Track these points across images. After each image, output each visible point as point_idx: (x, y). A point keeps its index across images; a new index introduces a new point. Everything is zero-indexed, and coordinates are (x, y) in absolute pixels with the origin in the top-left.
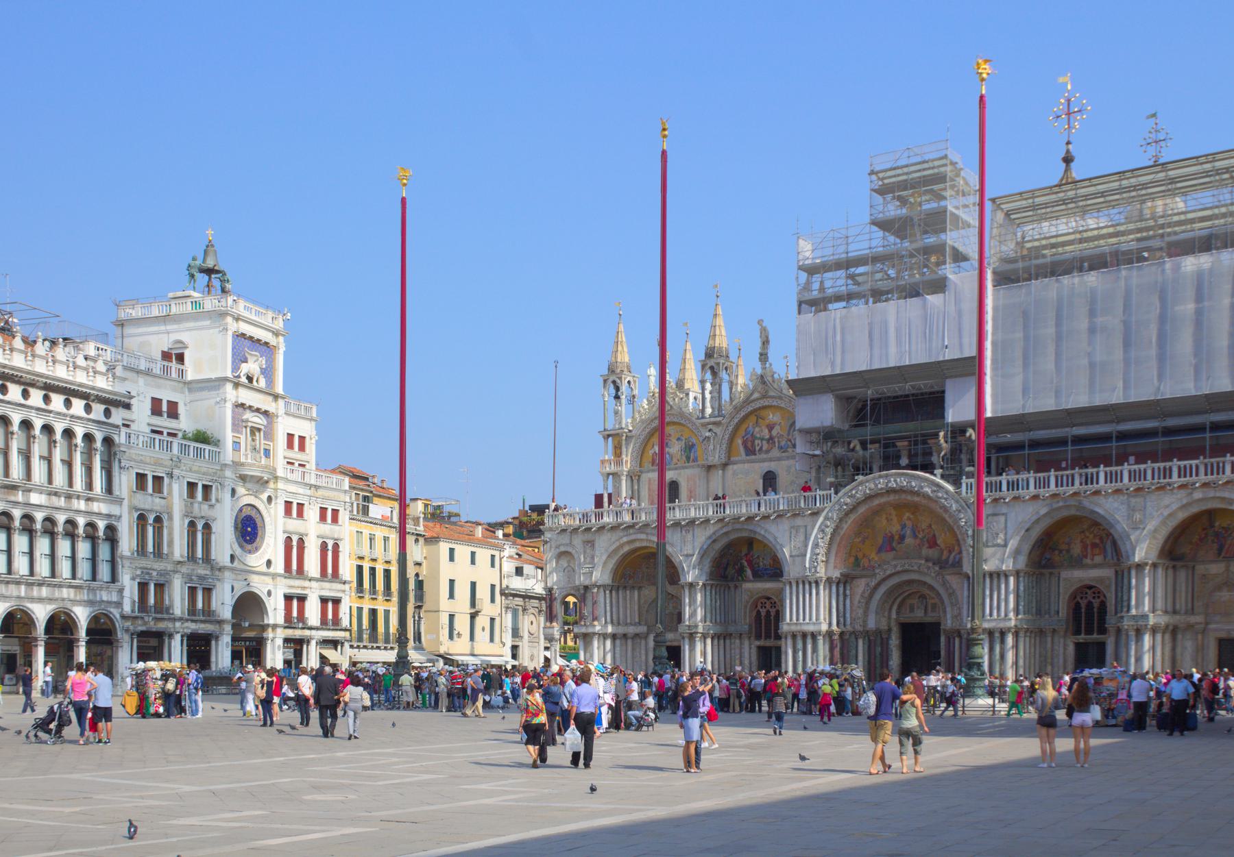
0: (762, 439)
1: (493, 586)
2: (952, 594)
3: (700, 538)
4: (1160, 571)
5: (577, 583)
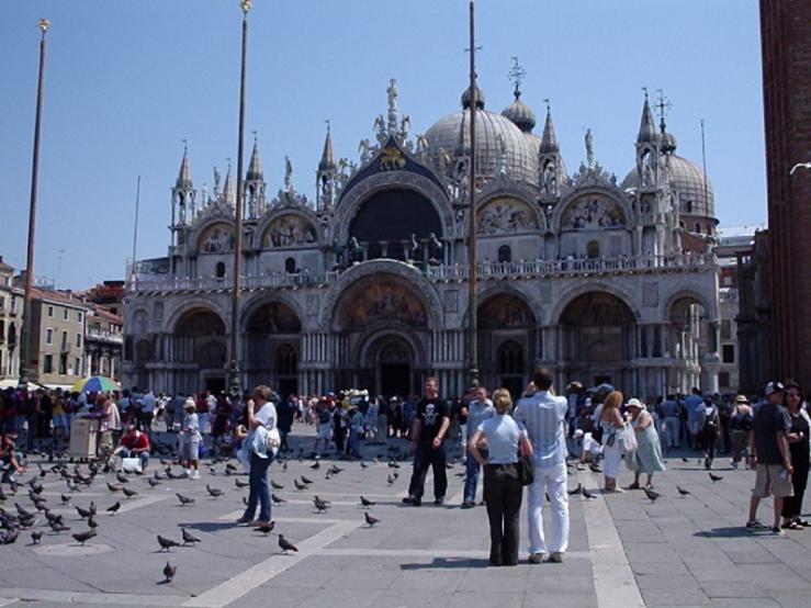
0: (285, 236)
1: (79, 336)
4: (561, 332)
5: (150, 331)
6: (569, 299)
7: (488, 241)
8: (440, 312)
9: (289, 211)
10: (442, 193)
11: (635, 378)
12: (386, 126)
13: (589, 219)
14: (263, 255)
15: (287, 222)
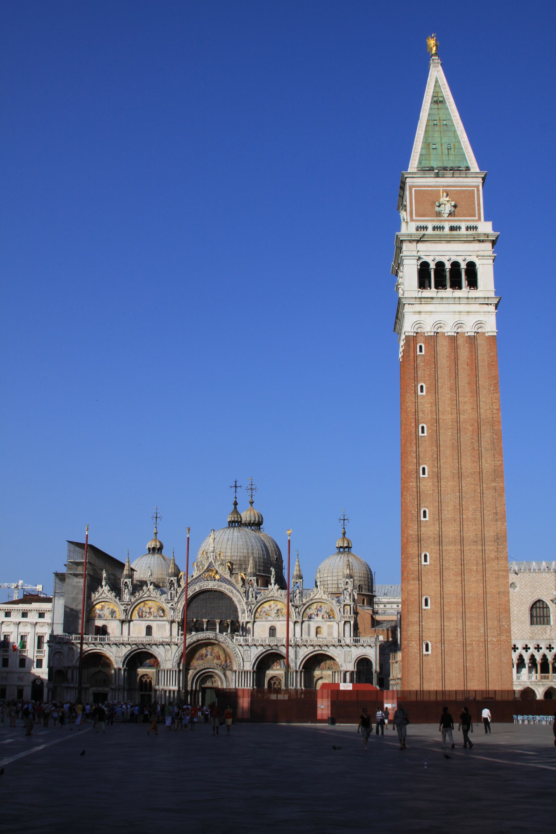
0: (146, 612)
3: (125, 650)
5: (65, 665)
7: (264, 623)
9: (149, 598)
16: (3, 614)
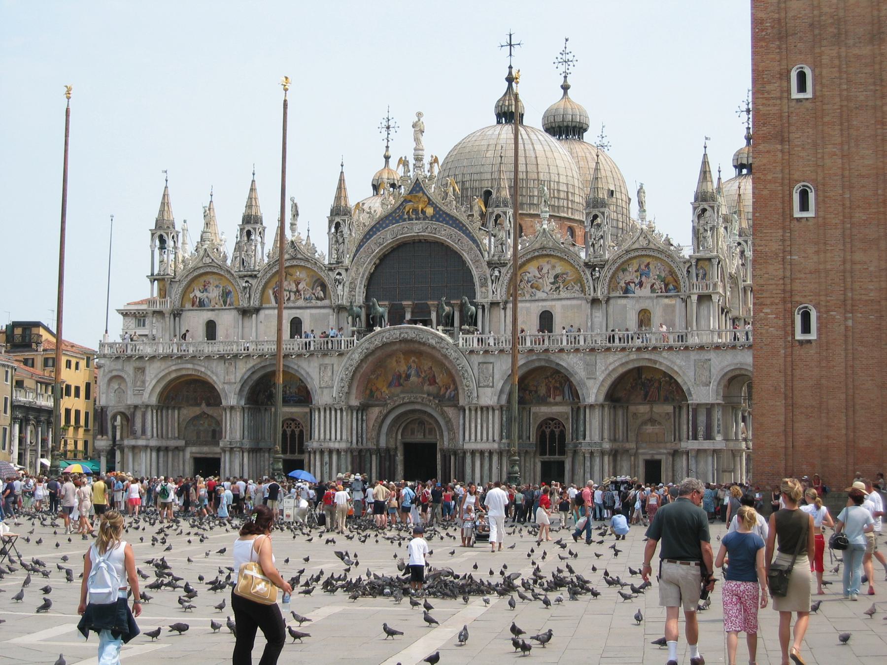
1: (6, 399)
2: (448, 421)
3: (242, 370)
4: (606, 409)
5: (129, 402)
6: (615, 376)
7: (528, 305)
8: (473, 386)
10: (474, 246)
11: (685, 462)
12: (411, 167)
13: (641, 284)
14: (262, 313)
15: (291, 275)
16: (132, 322)
